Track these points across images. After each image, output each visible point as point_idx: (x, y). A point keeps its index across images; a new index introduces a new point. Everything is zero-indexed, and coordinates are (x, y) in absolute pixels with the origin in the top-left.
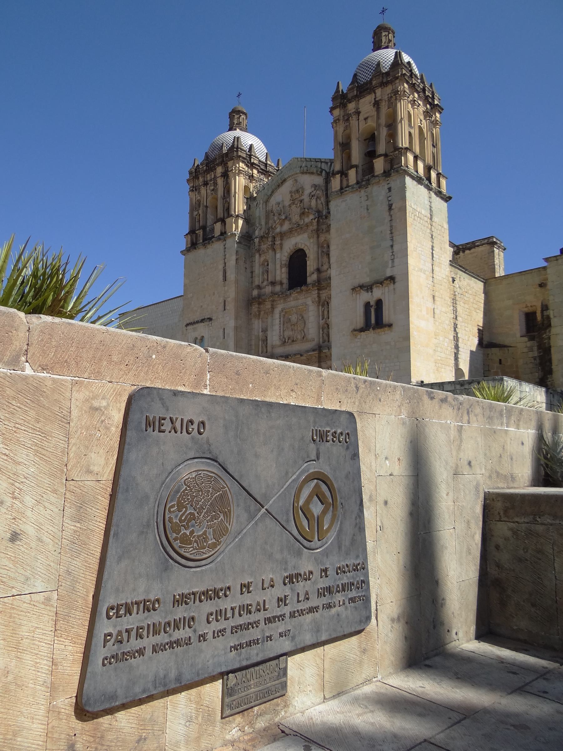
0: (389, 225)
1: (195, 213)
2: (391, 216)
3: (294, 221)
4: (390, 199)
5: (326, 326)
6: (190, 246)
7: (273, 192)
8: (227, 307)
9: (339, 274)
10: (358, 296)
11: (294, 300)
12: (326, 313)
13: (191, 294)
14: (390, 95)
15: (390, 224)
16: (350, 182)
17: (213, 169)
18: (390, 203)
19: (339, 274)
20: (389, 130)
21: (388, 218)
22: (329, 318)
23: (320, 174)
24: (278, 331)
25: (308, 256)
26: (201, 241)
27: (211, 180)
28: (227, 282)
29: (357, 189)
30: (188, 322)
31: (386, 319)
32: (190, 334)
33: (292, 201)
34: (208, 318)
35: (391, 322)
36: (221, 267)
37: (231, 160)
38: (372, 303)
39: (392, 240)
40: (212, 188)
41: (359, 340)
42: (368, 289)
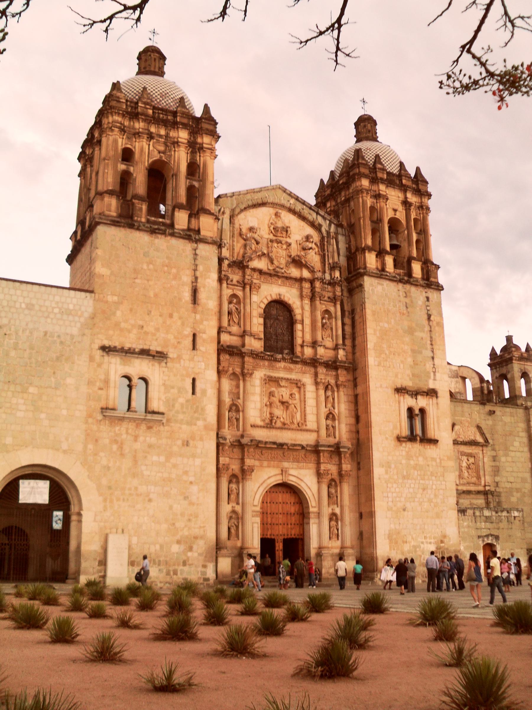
0: (429, 335)
1: (122, 167)
2: (431, 327)
3: (275, 262)
4: (428, 308)
5: (331, 416)
6: (114, 214)
7: (245, 208)
8: (202, 349)
9: (378, 365)
10: (402, 398)
11: (285, 368)
12: (331, 399)
13: (115, 298)
14: (417, 204)
15: (430, 334)
16: (387, 267)
17: (175, 125)
18: (429, 313)
19: (378, 365)
20: (418, 236)
21: (427, 328)
22: (334, 408)
23: (317, 228)
24: (258, 405)
25: (298, 317)
26: (143, 220)
27: (160, 136)
28: (199, 308)
29: (395, 281)
30: (107, 343)
31: (432, 433)
32: (113, 366)
33: (271, 237)
34: (158, 352)
35: (436, 438)
36: (187, 278)
37: (211, 135)
38: (417, 412)
39: (433, 352)
40: (162, 148)
41: (404, 449)
42: (412, 394)
